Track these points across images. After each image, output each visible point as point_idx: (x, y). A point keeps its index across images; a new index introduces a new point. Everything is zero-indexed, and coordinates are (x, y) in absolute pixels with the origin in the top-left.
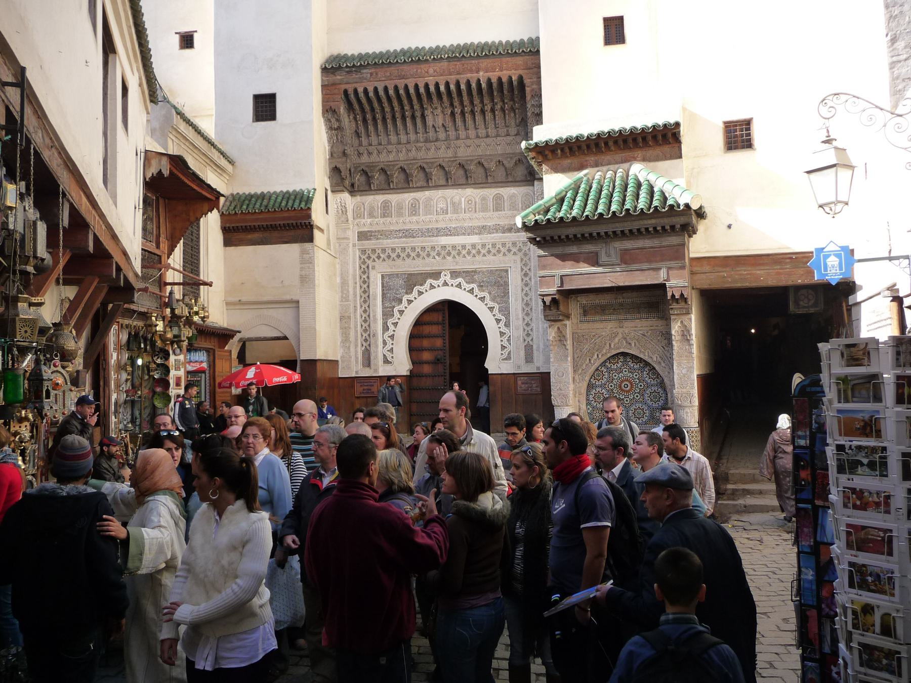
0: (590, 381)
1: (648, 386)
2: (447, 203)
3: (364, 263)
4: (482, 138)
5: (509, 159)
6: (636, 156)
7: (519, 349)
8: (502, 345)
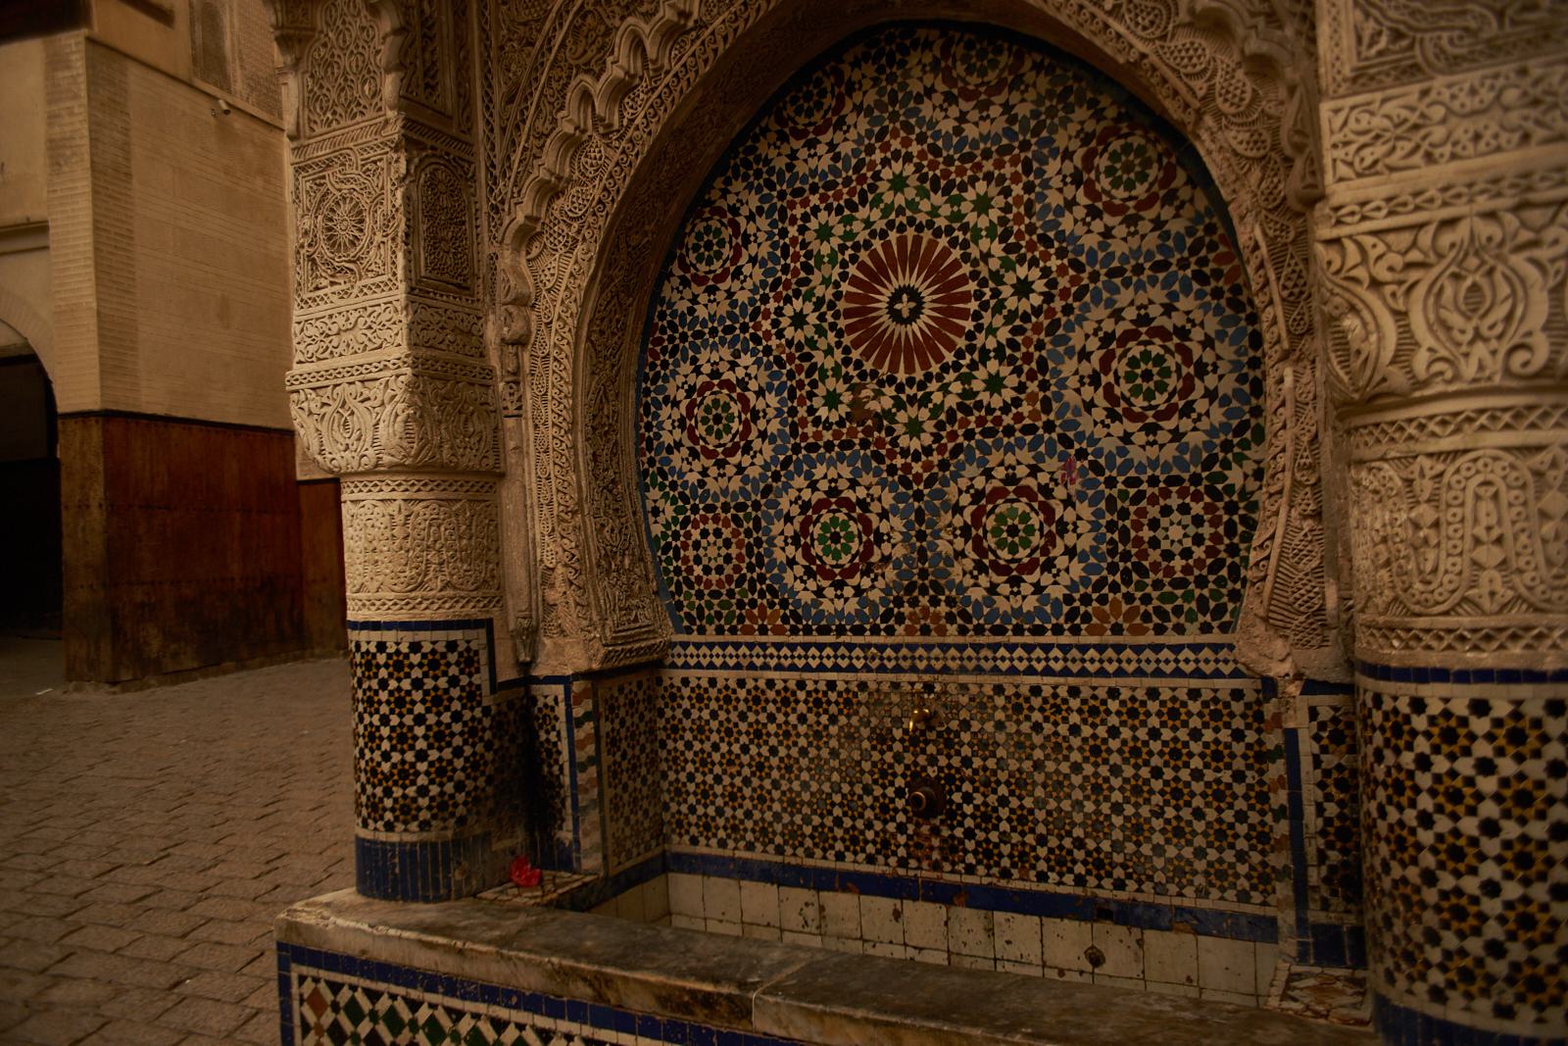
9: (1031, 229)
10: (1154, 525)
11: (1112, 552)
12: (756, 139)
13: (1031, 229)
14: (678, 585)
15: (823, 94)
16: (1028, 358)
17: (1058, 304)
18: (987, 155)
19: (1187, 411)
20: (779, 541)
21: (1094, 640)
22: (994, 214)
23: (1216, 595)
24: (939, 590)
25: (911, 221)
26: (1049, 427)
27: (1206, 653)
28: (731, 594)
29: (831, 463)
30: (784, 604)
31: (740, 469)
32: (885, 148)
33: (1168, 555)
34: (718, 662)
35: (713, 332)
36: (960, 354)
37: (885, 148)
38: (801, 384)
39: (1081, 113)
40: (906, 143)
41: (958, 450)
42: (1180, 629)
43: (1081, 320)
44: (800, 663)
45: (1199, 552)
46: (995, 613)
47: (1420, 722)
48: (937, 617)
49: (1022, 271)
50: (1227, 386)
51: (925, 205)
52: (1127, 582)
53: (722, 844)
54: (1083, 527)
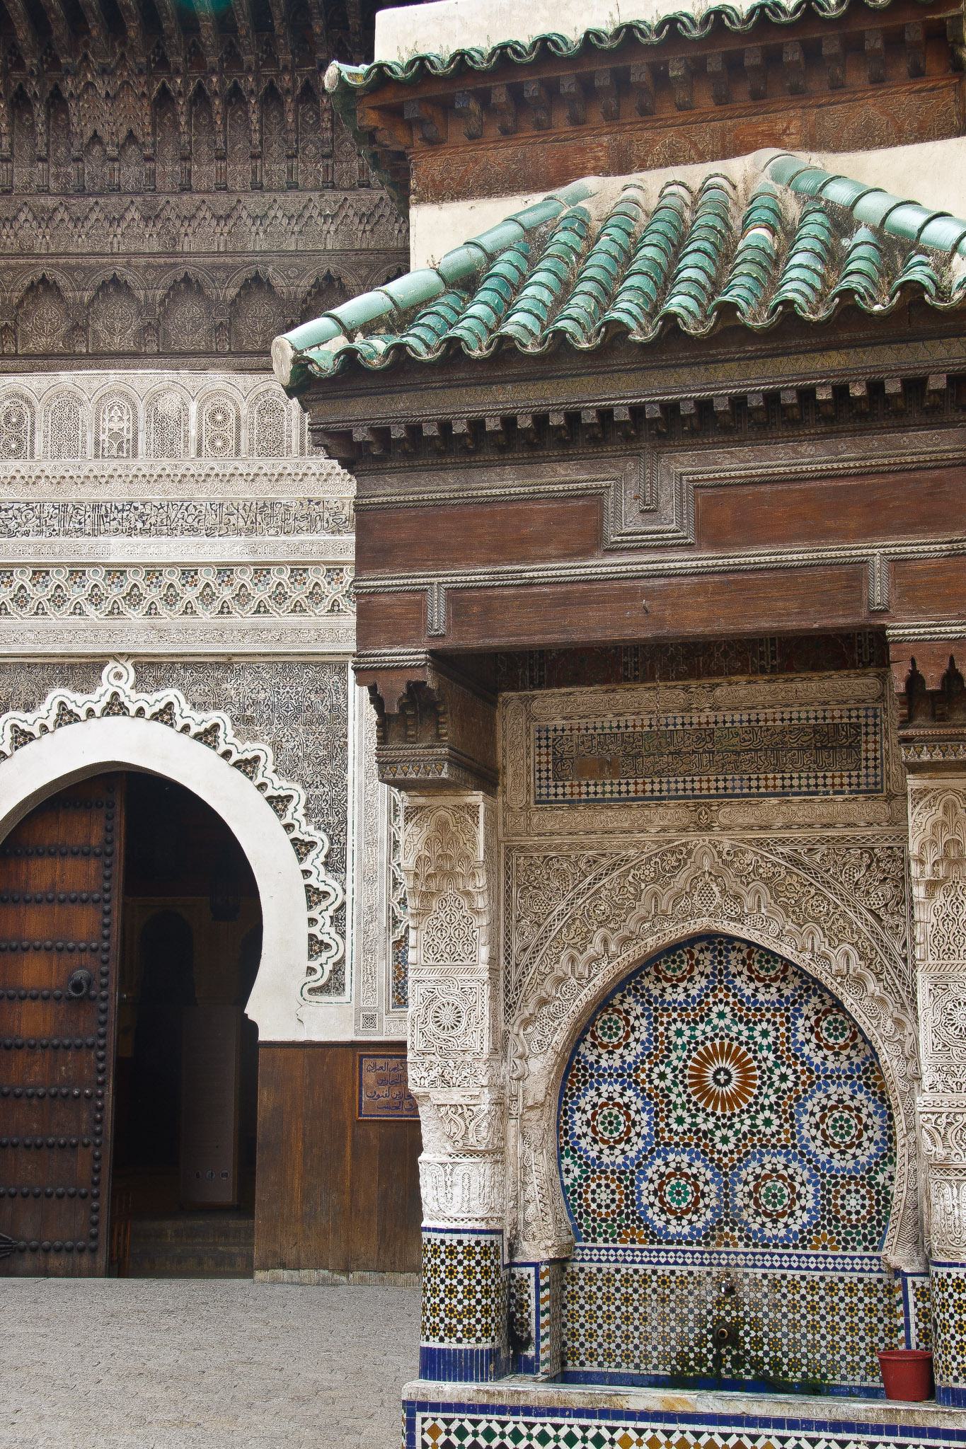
0: (575, 1051)
1: (816, 1078)
2: (135, 415)
4: (270, 190)
5: (363, 272)
6: (780, 127)
7: (372, 952)
8: (312, 937)
9: (789, 1050)
10: (843, 1198)
11: (823, 1210)
12: (642, 977)
13: (789, 1050)
14: (580, 1214)
15: (682, 962)
16: (785, 1112)
17: (800, 1088)
18: (768, 1010)
19: (860, 1145)
20: (645, 1193)
21: (814, 1252)
22: (771, 1040)
23: (871, 1233)
24: (735, 1224)
25: (727, 1036)
26: (794, 1146)
27: (866, 1260)
28: (614, 1220)
29: (678, 1153)
30: (646, 1227)
31: (623, 1152)
32: (715, 996)
33: (849, 1213)
34: (604, 1259)
35: (610, 1075)
36: (750, 1105)
37: (715, 996)
38: (662, 1110)
39: (815, 1000)
40: (726, 996)
41: (747, 1153)
42: (854, 1249)
43: (811, 1097)
44: (655, 1260)
45: (863, 1212)
46: (764, 1237)
47: (950, 1281)
48: (733, 1238)
49: (783, 1069)
50: (878, 1136)
51: (735, 1029)
52: (830, 1225)
53: (600, 1364)
54: (810, 1196)
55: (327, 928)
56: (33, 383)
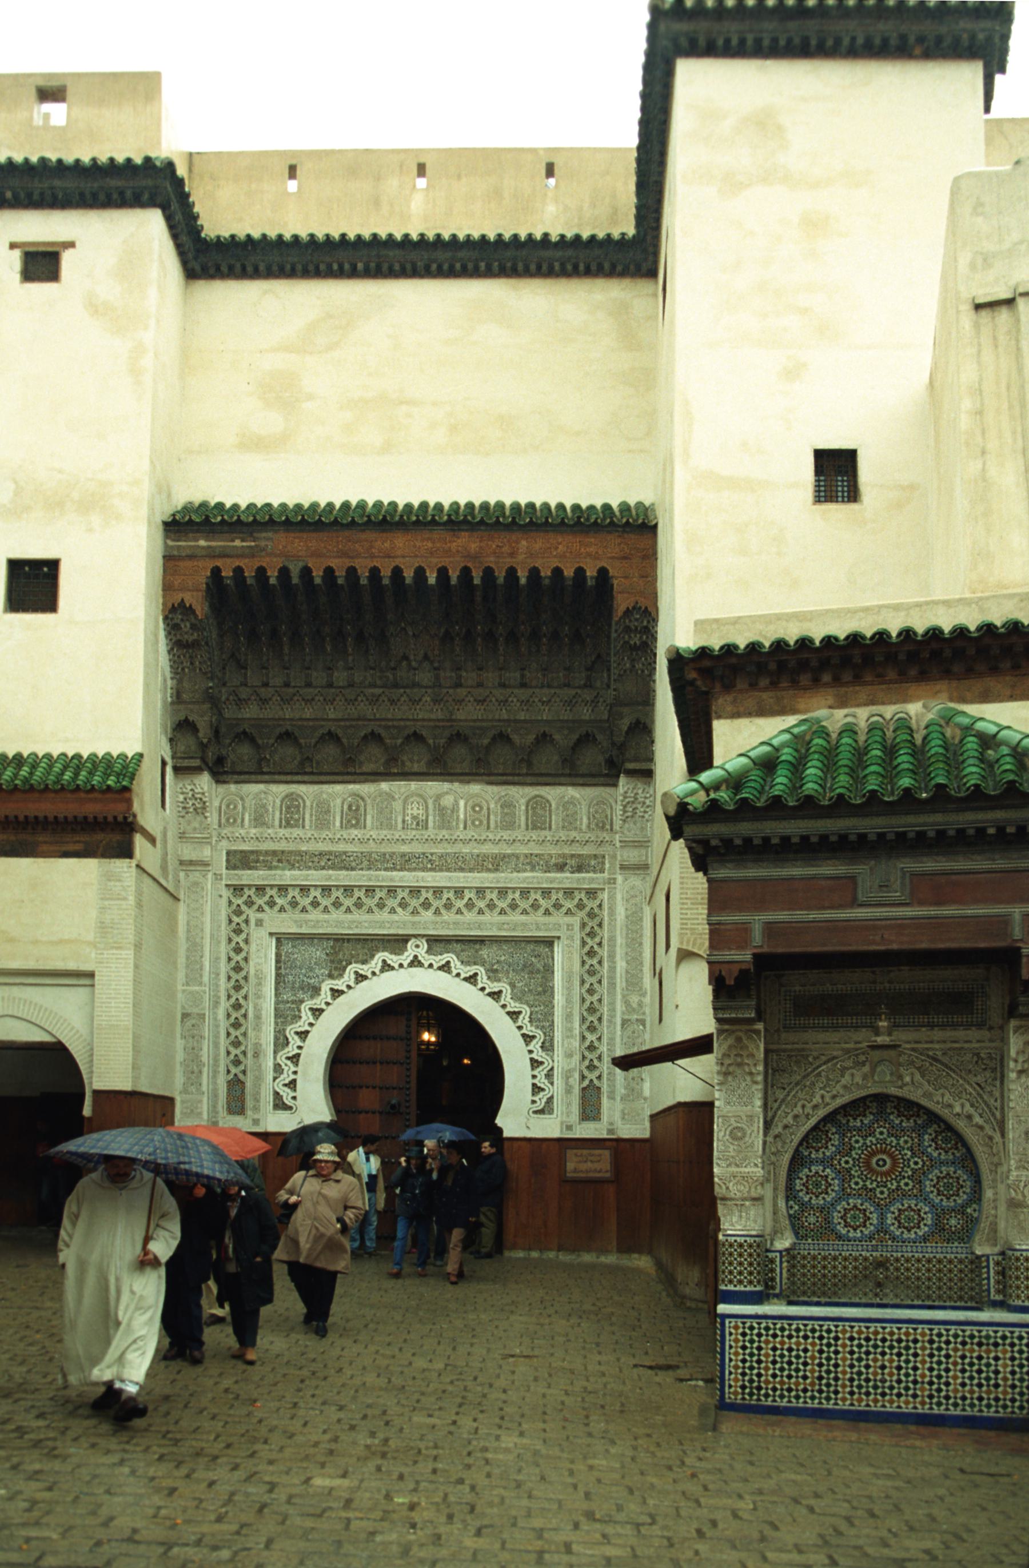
3: (238, 912)
55: (543, 1080)
56: (365, 789)
